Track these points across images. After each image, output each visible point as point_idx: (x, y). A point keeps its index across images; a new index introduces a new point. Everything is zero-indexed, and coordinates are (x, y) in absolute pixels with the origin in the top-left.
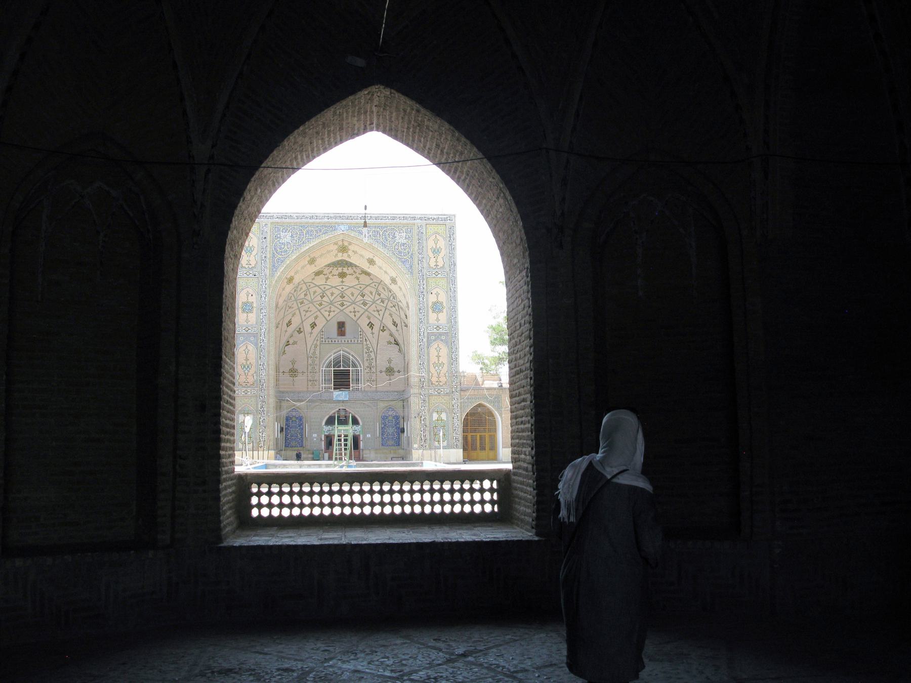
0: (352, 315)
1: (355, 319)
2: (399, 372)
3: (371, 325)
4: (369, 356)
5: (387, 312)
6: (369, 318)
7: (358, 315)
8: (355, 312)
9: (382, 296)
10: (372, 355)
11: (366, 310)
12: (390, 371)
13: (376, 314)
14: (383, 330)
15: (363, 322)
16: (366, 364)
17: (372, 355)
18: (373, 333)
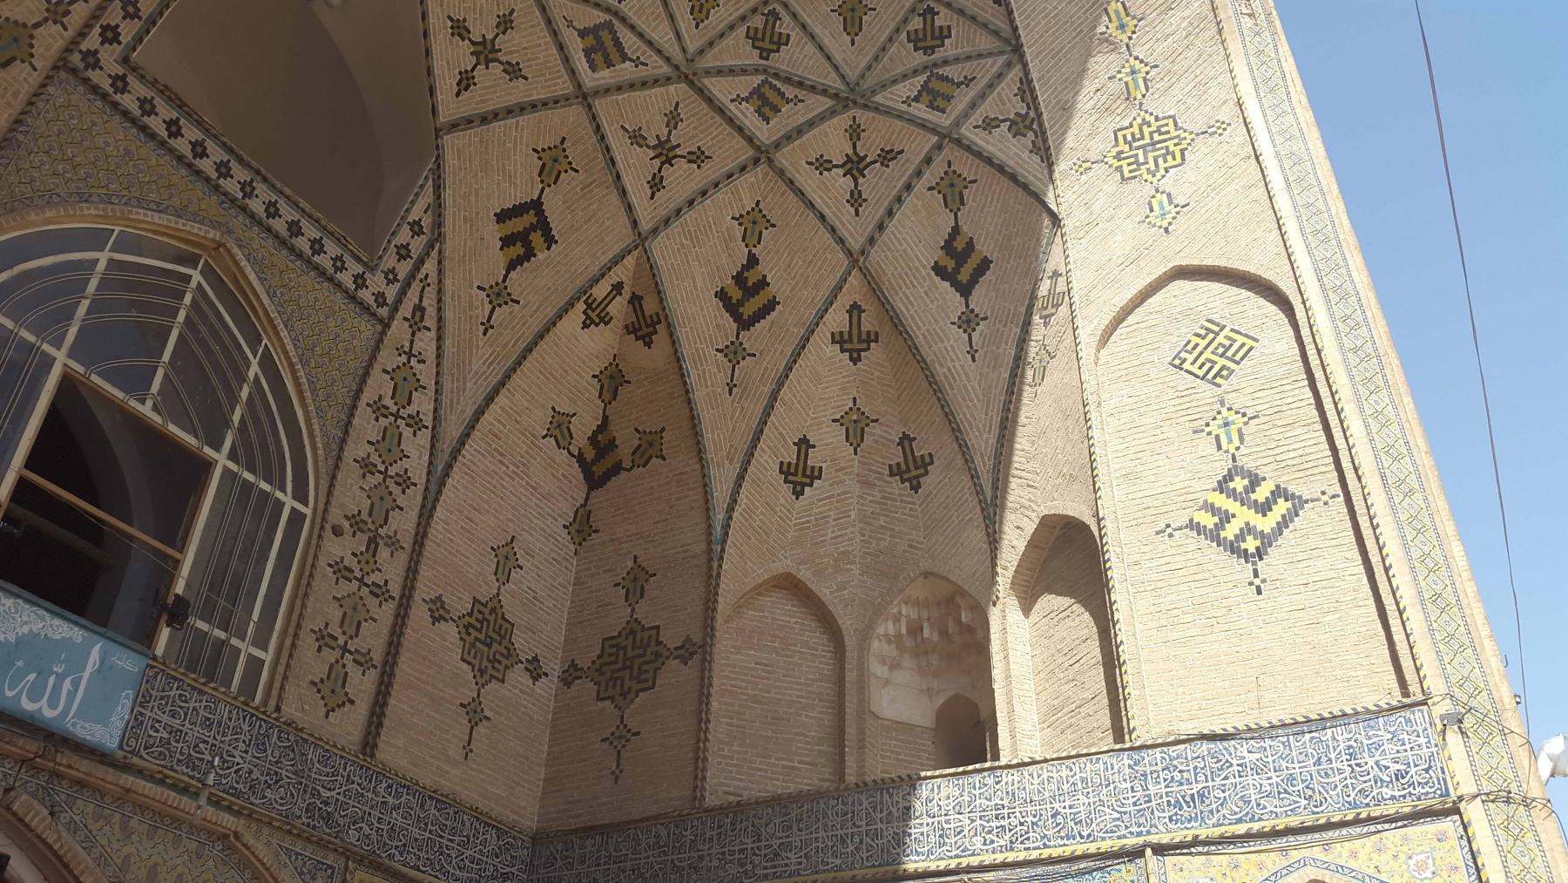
0: (449, 57)
1: (449, 106)
2: (535, 670)
3: (526, 230)
4: (389, 444)
5: (749, 189)
6: (552, 164)
7: (493, 89)
8: (485, 52)
9: (796, 58)
10: (416, 448)
11: (584, 97)
12: (488, 635)
13: (635, 165)
14: (596, 316)
15: (485, 174)
16: (352, 495)
17: (416, 448)
18: (499, 295)
